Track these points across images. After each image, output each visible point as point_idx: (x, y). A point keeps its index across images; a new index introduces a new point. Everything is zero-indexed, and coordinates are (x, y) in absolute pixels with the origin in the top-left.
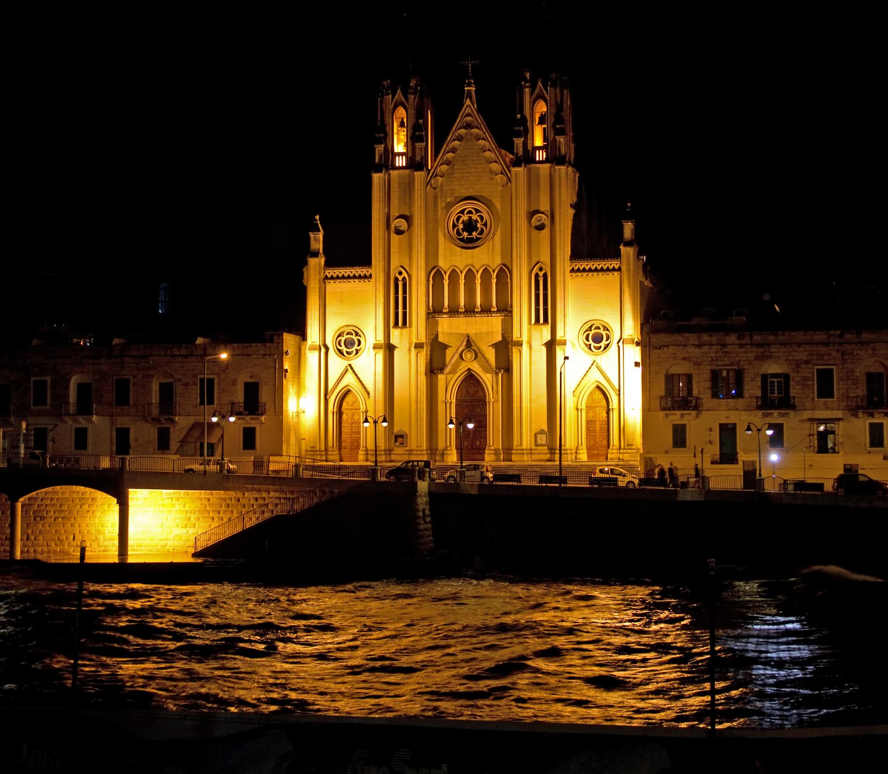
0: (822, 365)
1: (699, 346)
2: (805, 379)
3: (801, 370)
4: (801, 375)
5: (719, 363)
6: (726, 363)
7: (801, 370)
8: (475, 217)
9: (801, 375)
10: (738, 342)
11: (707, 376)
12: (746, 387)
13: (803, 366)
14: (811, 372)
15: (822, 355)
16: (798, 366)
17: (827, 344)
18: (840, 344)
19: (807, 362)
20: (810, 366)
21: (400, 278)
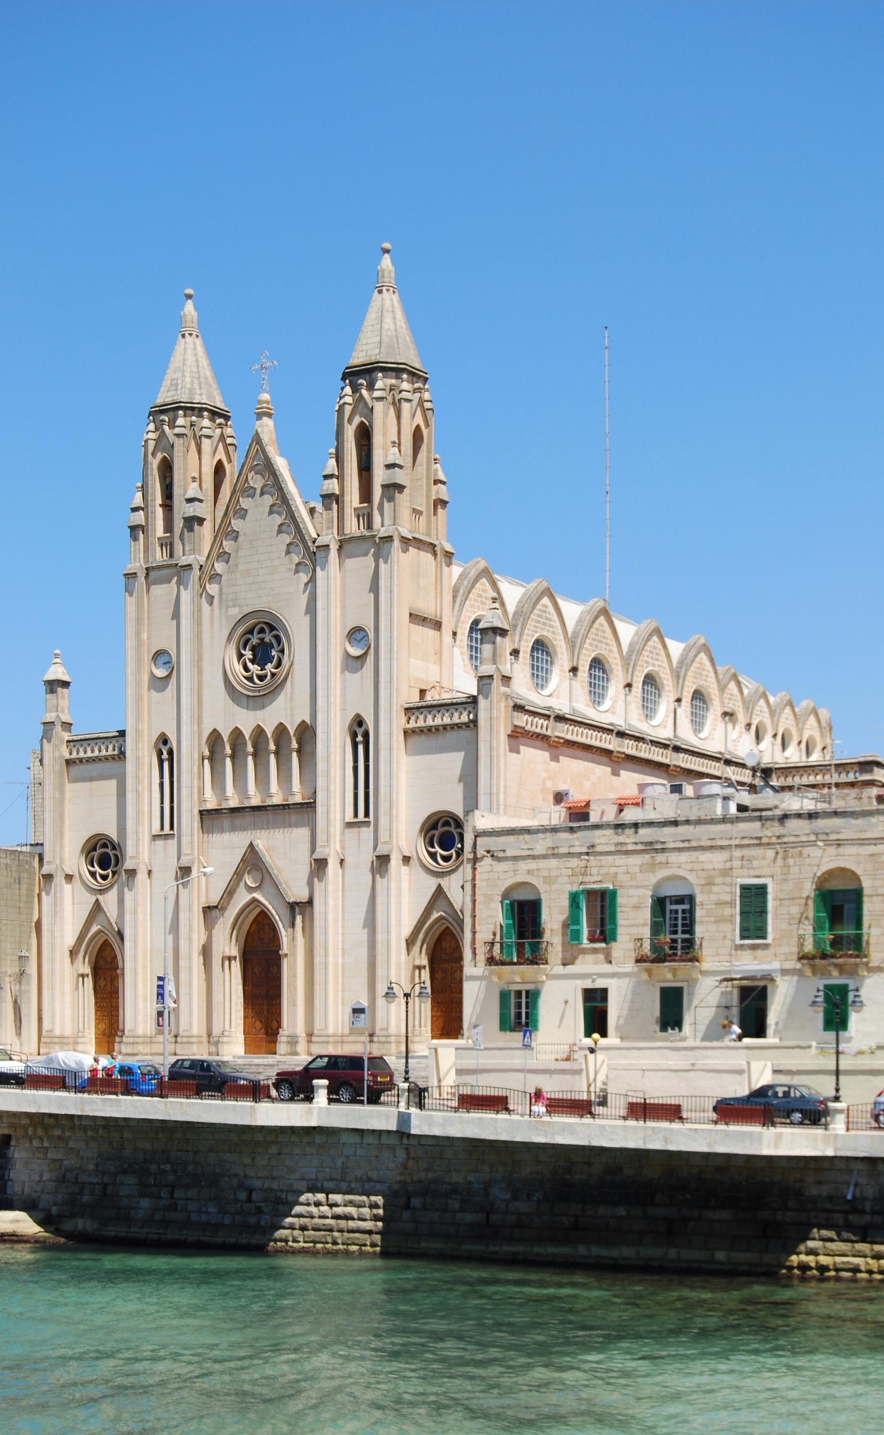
6: (599, 878)
7: (715, 889)
8: (268, 638)
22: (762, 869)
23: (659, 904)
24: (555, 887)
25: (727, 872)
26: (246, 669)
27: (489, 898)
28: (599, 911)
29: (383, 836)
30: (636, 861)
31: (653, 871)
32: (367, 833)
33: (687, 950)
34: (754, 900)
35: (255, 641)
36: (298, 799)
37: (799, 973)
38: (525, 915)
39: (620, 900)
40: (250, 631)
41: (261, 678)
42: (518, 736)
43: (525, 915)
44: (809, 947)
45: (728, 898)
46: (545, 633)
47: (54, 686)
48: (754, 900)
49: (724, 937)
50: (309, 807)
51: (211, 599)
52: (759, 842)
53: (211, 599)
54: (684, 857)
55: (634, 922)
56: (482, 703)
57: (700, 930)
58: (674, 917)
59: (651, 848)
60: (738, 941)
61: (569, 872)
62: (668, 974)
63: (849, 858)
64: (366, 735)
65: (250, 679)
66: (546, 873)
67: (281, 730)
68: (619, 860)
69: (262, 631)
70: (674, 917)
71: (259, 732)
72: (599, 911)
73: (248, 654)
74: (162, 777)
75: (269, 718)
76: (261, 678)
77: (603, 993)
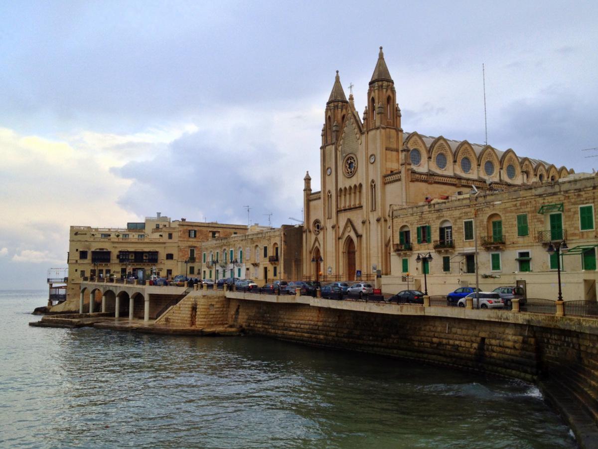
0: (467, 219)
1: (412, 215)
2: (460, 228)
3: (457, 223)
4: (457, 226)
5: (420, 223)
7: (457, 223)
8: (352, 161)
9: (457, 226)
10: (428, 210)
11: (416, 231)
12: (432, 236)
13: (458, 221)
14: (461, 224)
15: (467, 213)
16: (456, 221)
17: (469, 206)
18: (475, 205)
19: (460, 218)
20: (461, 220)
21: (330, 195)
24: (413, 226)
26: (348, 170)
27: (396, 232)
28: (424, 234)
31: (439, 219)
34: (468, 226)
35: (349, 162)
39: (432, 229)
40: (348, 160)
41: (351, 172)
42: (412, 181)
45: (461, 226)
46: (442, 152)
48: (468, 226)
49: (461, 239)
50: (361, 207)
60: (464, 240)
61: (417, 221)
65: (348, 173)
66: (410, 222)
67: (355, 186)
69: (351, 159)
71: (350, 187)
72: (424, 234)
73: (348, 166)
74: (329, 204)
76: (351, 172)
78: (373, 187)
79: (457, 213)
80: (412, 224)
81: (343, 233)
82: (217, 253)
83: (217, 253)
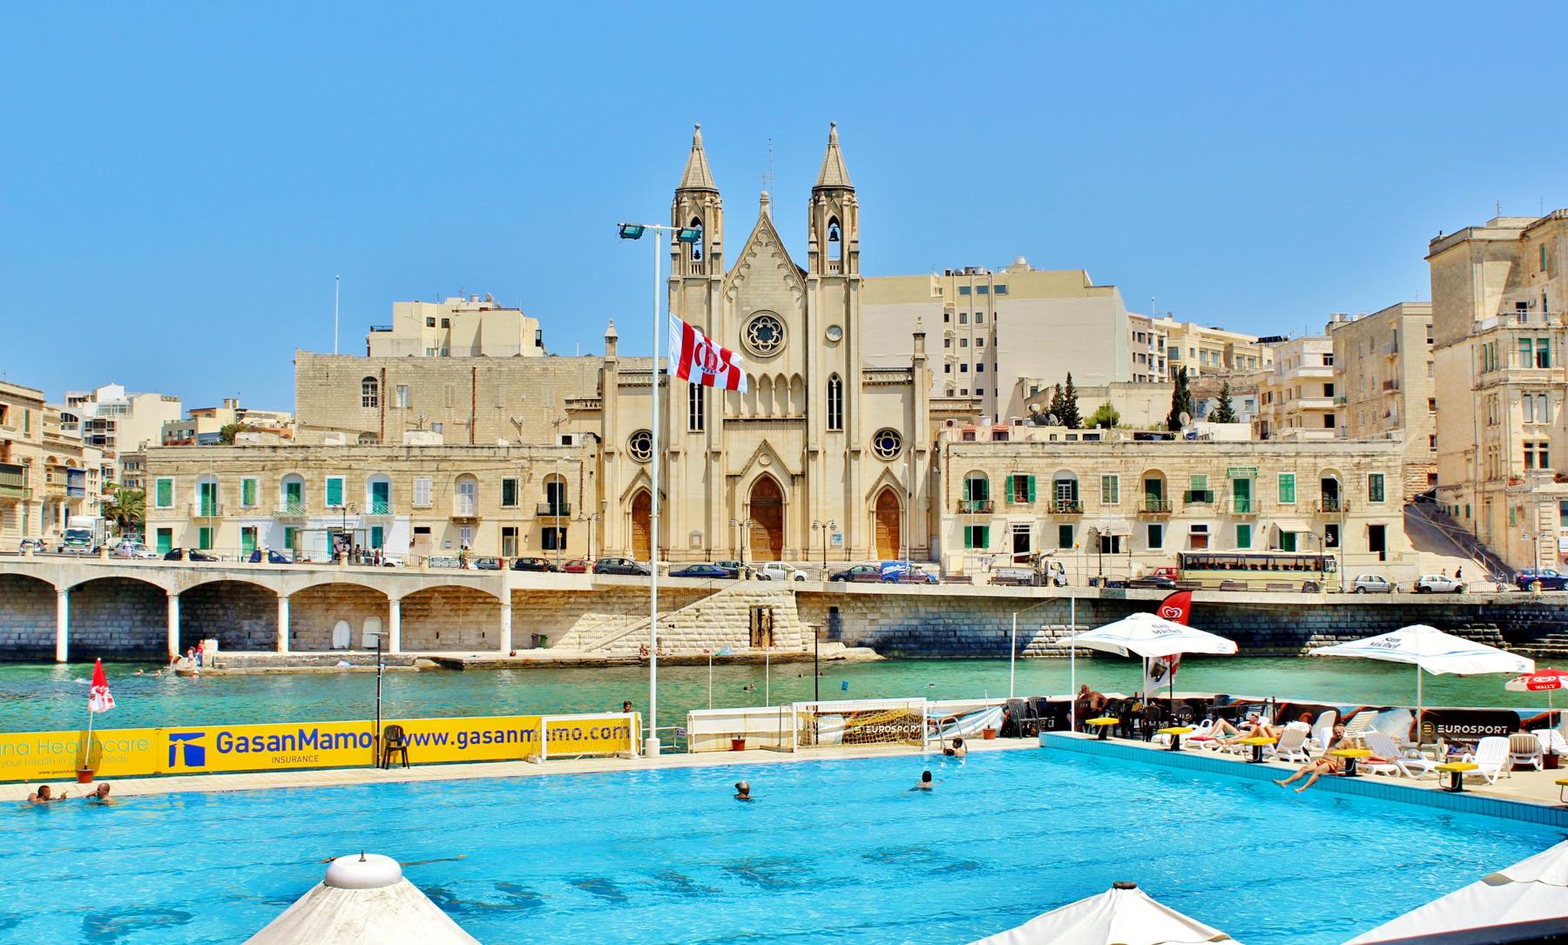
22: (1113, 467)
23: (1058, 483)
25: (1094, 470)
28: (1022, 487)
29: (854, 439)
30: (1045, 461)
32: (842, 438)
33: (1075, 508)
36: (792, 415)
37: (1137, 519)
38: (978, 489)
40: (757, 320)
43: (978, 489)
44: (1143, 507)
47: (611, 340)
51: (730, 300)
52: (1112, 455)
53: (730, 300)
54: (1071, 460)
55: (1043, 493)
56: (918, 371)
57: (1080, 498)
58: (1067, 492)
59: (1052, 455)
62: (1066, 520)
63: (1158, 464)
64: (839, 385)
67: (781, 376)
68: (1035, 460)
70: (1067, 492)
71: (765, 376)
73: (755, 333)
75: (773, 369)
77: (1026, 528)
78: (835, 388)
79: (1089, 462)
80: (994, 470)
81: (747, 468)
82: (248, 485)
83: (248, 485)
